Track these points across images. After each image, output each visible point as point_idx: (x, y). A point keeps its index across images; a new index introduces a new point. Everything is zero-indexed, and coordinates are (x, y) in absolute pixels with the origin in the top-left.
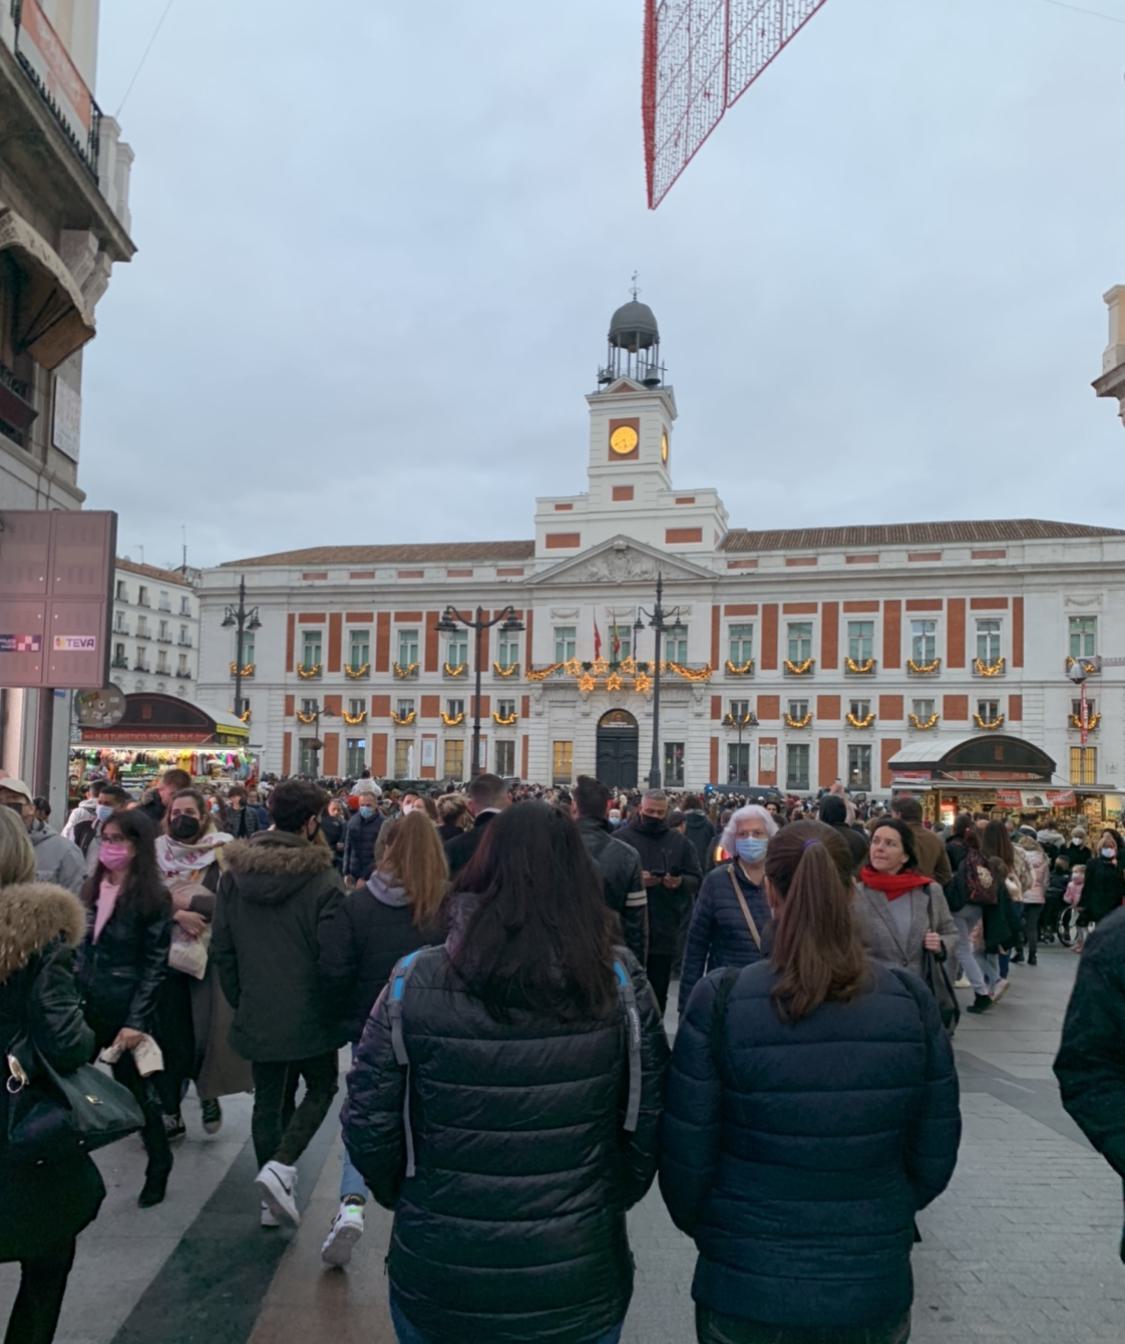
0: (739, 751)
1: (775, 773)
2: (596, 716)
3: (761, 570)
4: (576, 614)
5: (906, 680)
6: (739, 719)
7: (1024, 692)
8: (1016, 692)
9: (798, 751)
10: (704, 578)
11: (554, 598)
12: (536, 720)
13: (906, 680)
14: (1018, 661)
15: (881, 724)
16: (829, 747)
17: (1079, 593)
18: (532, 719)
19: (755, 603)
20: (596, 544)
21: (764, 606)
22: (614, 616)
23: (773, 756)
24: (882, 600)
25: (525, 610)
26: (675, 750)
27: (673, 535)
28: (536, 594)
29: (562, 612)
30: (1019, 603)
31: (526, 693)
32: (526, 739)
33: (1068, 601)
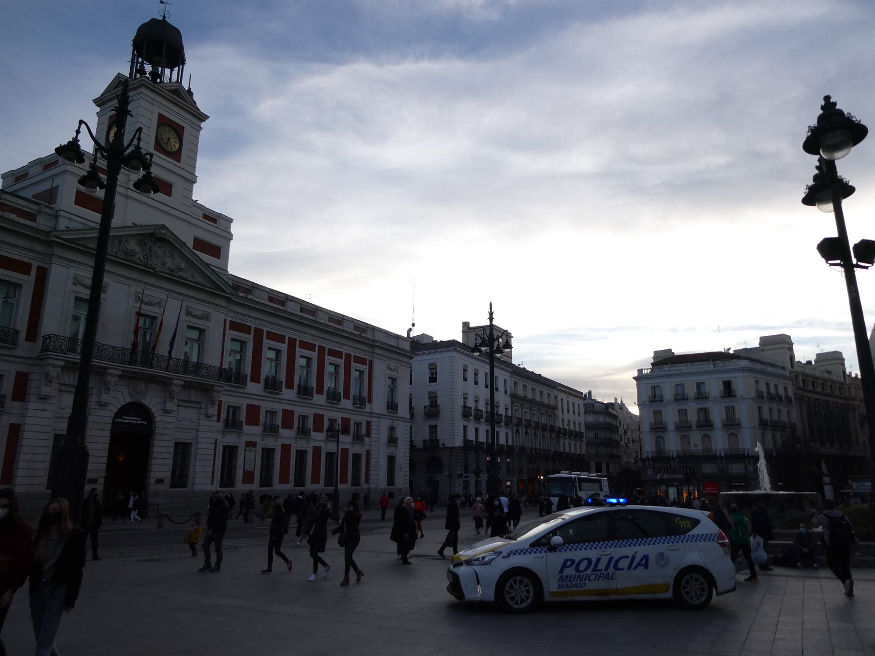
0: (230, 452)
1: (253, 473)
2: (113, 409)
3: (250, 297)
5: (325, 403)
6: (232, 424)
7: (374, 419)
8: (369, 419)
9: (268, 453)
10: (224, 291)
11: (80, 263)
12: (40, 406)
13: (325, 403)
14: (370, 401)
15: (246, 428)
16: (286, 448)
17: (393, 364)
18: (34, 405)
19: (249, 324)
20: (138, 223)
21: (255, 328)
22: (142, 302)
23: (253, 457)
24: (317, 344)
25: (35, 265)
26: (183, 451)
27: (199, 244)
28: (58, 251)
30: (371, 362)
31: (24, 369)
33: (389, 368)
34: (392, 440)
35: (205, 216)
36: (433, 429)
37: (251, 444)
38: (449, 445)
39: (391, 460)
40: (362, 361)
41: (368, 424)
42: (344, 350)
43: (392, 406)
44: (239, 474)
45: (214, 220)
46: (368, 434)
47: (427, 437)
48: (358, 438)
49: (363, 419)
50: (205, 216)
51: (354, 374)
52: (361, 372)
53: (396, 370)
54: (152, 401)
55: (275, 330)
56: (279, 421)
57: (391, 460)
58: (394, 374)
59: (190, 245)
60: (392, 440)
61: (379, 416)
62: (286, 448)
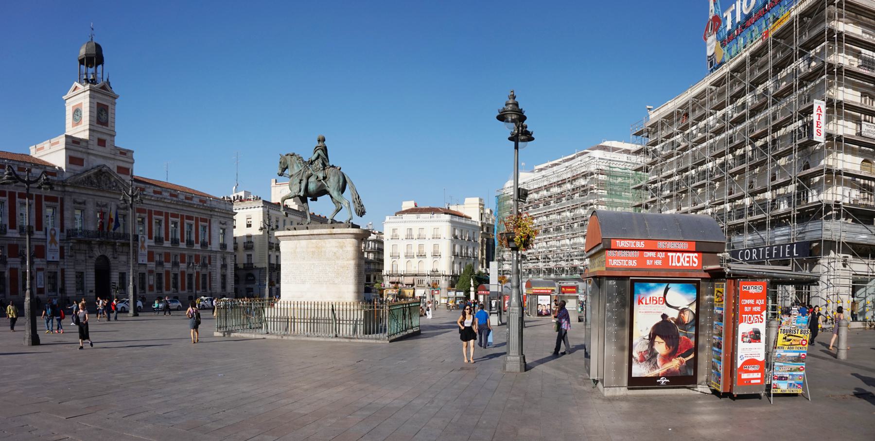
4: (84, 203)
32: (63, 271)
34: (224, 266)
35: (121, 153)
36: (249, 256)
38: (259, 266)
39: (224, 277)
40: (205, 220)
41: (210, 257)
42: (195, 215)
44: (147, 288)
45: (125, 154)
46: (210, 263)
47: (246, 262)
48: (204, 265)
49: (206, 254)
50: (121, 153)
51: (200, 228)
52: (204, 227)
53: (225, 224)
54: (109, 254)
55: (158, 209)
56: (163, 259)
57: (224, 277)
58: (224, 226)
59: (115, 170)
60: (224, 266)
61: (216, 252)
62: (168, 273)
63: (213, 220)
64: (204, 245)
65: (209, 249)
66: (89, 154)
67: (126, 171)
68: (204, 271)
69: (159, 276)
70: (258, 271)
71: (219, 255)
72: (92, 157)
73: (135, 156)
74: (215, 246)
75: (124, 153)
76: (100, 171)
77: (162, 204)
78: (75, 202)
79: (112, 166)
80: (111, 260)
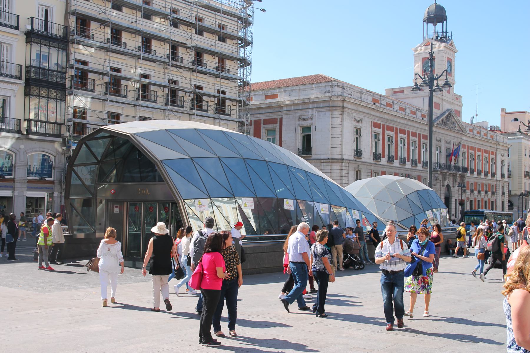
29: (438, 139)
37: (468, 199)
39: (503, 203)
40: (493, 153)
42: (489, 149)
43: (503, 176)
58: (503, 158)
63: (498, 152)
64: (493, 175)
65: (495, 179)
66: (443, 99)
67: (458, 113)
68: (493, 199)
69: (471, 201)
70: (517, 198)
71: (501, 184)
72: (444, 103)
73: (463, 100)
74: (498, 176)
75: (458, 98)
76: (450, 114)
77: (473, 140)
78: (437, 140)
79: (454, 108)
80: (452, 188)
